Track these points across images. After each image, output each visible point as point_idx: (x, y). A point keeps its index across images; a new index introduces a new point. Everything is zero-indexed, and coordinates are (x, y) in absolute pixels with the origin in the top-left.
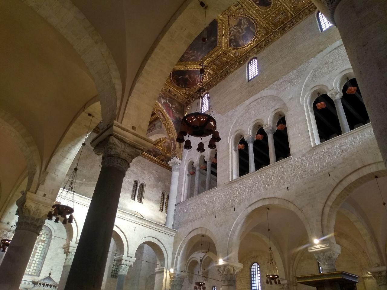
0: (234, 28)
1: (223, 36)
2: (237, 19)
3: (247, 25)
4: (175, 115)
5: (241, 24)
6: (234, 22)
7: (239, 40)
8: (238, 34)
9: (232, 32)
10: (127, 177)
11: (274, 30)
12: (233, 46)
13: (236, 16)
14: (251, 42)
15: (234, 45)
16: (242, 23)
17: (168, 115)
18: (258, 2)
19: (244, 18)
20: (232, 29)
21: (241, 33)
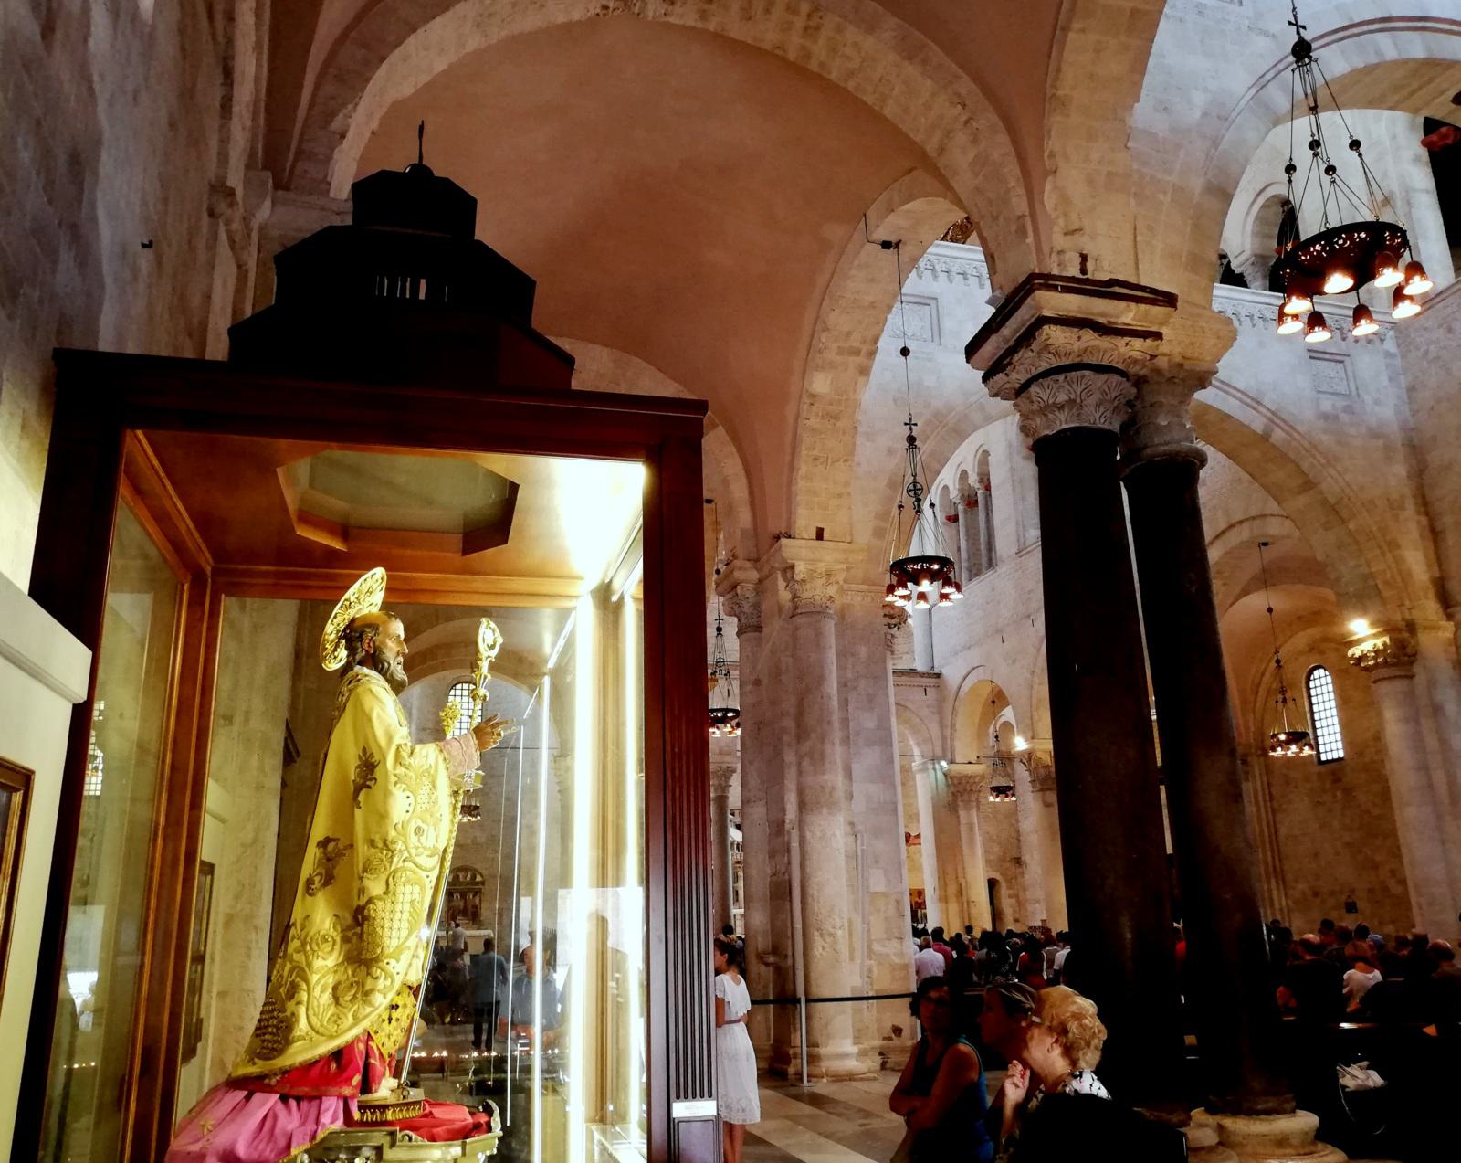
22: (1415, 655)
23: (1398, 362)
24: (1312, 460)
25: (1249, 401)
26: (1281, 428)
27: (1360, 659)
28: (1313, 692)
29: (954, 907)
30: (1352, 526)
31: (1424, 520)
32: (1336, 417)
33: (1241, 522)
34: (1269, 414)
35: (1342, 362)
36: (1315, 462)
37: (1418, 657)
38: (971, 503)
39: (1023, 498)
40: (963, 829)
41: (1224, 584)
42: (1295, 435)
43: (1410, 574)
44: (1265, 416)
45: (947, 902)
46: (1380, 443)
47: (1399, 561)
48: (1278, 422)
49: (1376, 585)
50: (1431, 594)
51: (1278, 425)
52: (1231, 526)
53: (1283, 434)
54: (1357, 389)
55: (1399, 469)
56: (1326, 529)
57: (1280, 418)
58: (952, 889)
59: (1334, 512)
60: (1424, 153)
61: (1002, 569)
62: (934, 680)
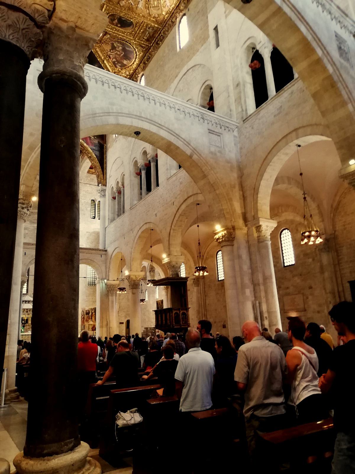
0: (110, 52)
1: (104, 61)
2: (108, 44)
3: (121, 46)
4: (94, 141)
5: (116, 47)
6: (108, 48)
7: (122, 61)
8: (117, 56)
9: (111, 56)
10: (83, 198)
11: (150, 45)
12: (119, 67)
13: (106, 41)
14: (134, 60)
15: (120, 66)
16: (116, 46)
17: (85, 145)
18: (119, 25)
19: (115, 42)
20: (109, 53)
21: (120, 55)
22: (234, 238)
23: (238, 139)
24: (206, 167)
25: (186, 143)
26: (197, 155)
27: (218, 239)
28: (218, 259)
29: (105, 329)
30: (217, 192)
31: (241, 193)
32: (215, 154)
33: (191, 196)
34: (192, 149)
35: (220, 136)
36: (207, 168)
37: (235, 238)
38: (119, 192)
39: (133, 190)
40: (110, 302)
41: (187, 218)
42: (202, 158)
43: (235, 210)
44: (191, 149)
45: (102, 328)
46: (229, 165)
47: (232, 205)
48: (196, 152)
49: (224, 213)
50: (241, 218)
51: (196, 154)
52: (188, 197)
53: (197, 157)
54: (224, 146)
55: (235, 175)
56: (210, 193)
57: (196, 150)
58: (105, 323)
59: (213, 187)
60: (249, 70)
61: (126, 214)
62: (105, 252)
